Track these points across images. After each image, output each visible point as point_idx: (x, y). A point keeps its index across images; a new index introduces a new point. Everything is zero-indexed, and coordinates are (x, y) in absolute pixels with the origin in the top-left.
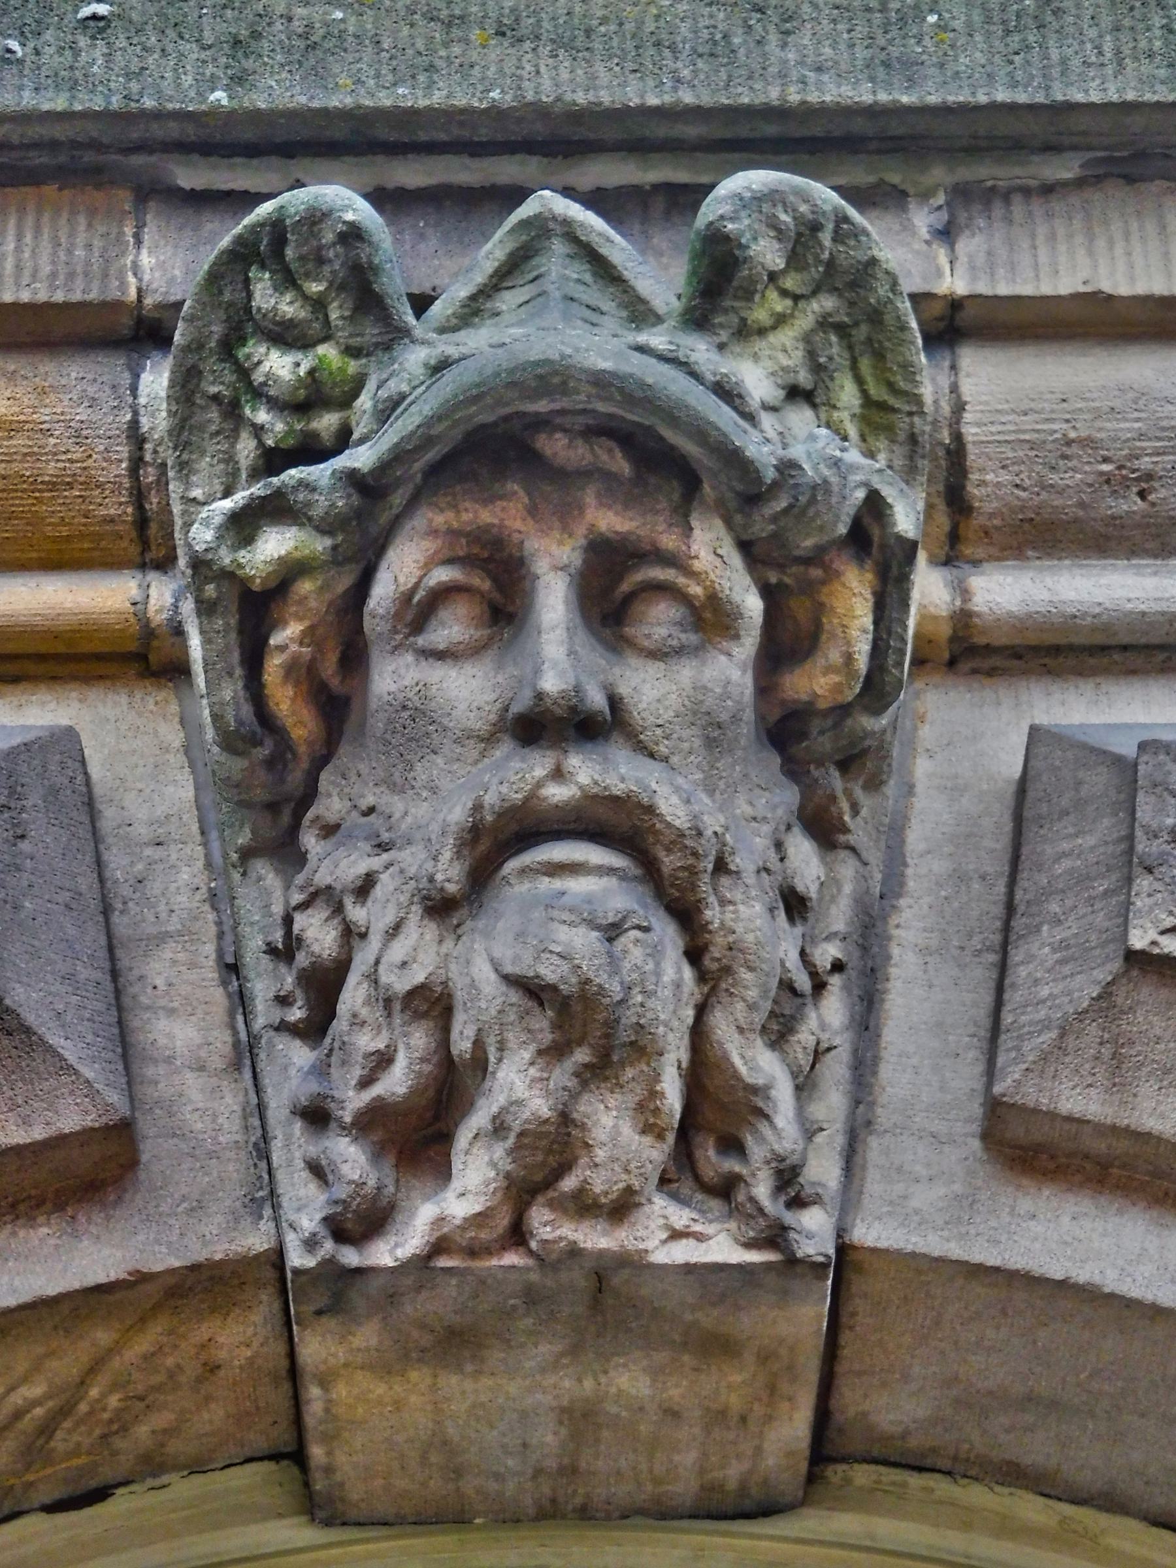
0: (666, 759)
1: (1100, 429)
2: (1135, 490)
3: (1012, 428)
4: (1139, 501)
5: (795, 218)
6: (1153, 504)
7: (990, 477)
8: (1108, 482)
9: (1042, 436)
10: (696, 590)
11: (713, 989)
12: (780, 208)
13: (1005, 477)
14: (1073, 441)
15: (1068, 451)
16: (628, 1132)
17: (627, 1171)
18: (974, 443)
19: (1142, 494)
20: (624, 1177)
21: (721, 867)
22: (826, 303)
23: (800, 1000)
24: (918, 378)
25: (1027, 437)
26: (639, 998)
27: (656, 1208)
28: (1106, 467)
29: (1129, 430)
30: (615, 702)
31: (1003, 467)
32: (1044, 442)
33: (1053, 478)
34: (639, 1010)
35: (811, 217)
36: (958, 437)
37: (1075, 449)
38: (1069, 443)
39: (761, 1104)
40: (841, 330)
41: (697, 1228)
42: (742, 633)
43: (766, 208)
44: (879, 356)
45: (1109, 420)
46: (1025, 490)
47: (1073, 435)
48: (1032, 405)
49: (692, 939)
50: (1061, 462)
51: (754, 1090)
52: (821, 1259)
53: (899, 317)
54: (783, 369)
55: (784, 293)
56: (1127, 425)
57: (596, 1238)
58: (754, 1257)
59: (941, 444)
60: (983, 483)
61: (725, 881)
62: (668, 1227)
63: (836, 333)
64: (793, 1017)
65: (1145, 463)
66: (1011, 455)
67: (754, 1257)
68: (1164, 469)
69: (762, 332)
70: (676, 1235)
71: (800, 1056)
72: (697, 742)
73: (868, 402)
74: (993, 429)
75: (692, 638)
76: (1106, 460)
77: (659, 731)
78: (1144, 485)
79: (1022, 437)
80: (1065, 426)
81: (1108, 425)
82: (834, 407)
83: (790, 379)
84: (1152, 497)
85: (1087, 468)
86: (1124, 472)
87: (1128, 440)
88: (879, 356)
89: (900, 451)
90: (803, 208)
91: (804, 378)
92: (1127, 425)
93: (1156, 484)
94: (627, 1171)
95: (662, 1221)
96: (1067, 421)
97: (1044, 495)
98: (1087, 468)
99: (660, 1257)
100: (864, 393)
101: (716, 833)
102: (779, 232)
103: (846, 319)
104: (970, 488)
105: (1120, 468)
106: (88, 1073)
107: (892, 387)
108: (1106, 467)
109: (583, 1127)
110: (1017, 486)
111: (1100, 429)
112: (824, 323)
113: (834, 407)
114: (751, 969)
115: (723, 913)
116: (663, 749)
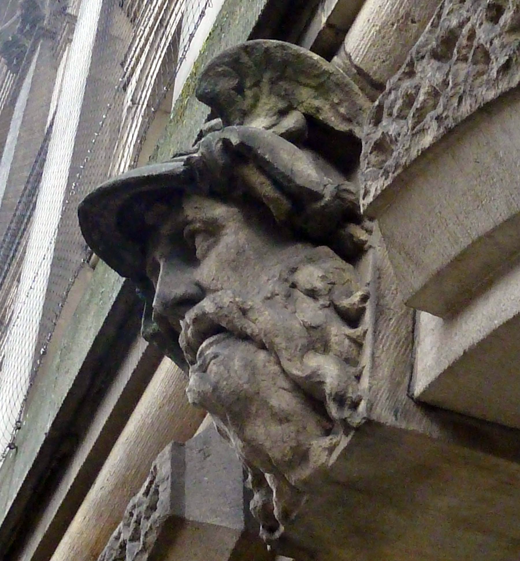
0: (222, 289)
1: (382, 18)
2: (409, 23)
3: (364, 47)
4: (414, 24)
5: (226, 65)
6: (419, 21)
7: (375, 68)
8: (401, 30)
9: (372, 39)
10: (198, 225)
11: (275, 353)
12: (216, 67)
13: (377, 63)
14: (380, 30)
15: (382, 34)
16: (276, 429)
17: (284, 442)
18: (361, 63)
19: (413, 22)
20: (286, 445)
21: (244, 312)
22: (267, 76)
23: (320, 328)
24: (319, 66)
25: (369, 44)
26: (225, 383)
27: (314, 445)
28: (395, 27)
29: (388, 8)
30: (198, 284)
31: (374, 61)
32: (374, 40)
33: (388, 47)
34: (228, 387)
35: (231, 59)
36: (356, 67)
37: (383, 32)
38: (379, 31)
39: (318, 380)
40: (280, 78)
41: (334, 441)
42: (224, 224)
43: (211, 74)
44: (303, 72)
45: (382, 11)
46: (387, 60)
47: (378, 28)
48: (363, 32)
49: (256, 342)
50: (384, 40)
51: (308, 377)
52: (364, 421)
53: (294, 55)
54: (269, 110)
55: (250, 88)
56: (387, 6)
57: (304, 473)
58: (350, 437)
59: (355, 74)
60: (375, 73)
61: (250, 314)
62: (325, 449)
63: (281, 81)
64: (322, 336)
65: (402, 12)
66: (372, 55)
67: (350, 437)
68: (408, 7)
69: (254, 106)
70: (331, 450)
71: (337, 347)
72: (230, 273)
73: (316, 88)
74: (361, 53)
75: (212, 240)
76: (393, 25)
77: (214, 281)
78: (410, 18)
79: (368, 46)
80: (374, 28)
81: (383, 13)
82: (302, 102)
83: (275, 110)
84: (416, 19)
85: (391, 33)
86: (401, 22)
87: (391, 11)
88: (303, 72)
89: (338, 92)
90: (227, 59)
91: (281, 105)
92: (387, 6)
93: (412, 14)
94: (284, 442)
95: (320, 449)
96: (374, 26)
97: (392, 55)
98: (391, 33)
99: (331, 462)
100: (311, 87)
101: (231, 302)
102: (224, 74)
103: (279, 73)
104: (374, 78)
105: (398, 21)
106: (224, 524)
107: (317, 76)
108: (395, 27)
109: (254, 440)
110: (384, 62)
111: (382, 18)
112: (273, 82)
113: (302, 102)
114: (276, 336)
115: (256, 325)
116: (219, 286)
